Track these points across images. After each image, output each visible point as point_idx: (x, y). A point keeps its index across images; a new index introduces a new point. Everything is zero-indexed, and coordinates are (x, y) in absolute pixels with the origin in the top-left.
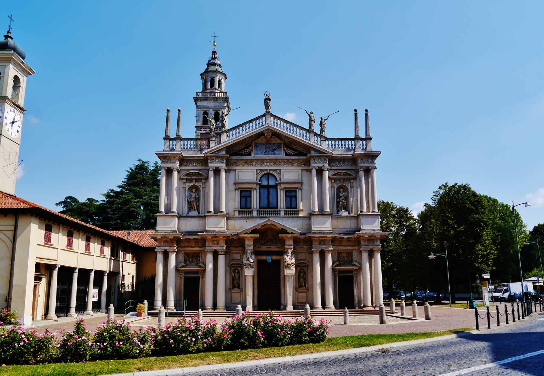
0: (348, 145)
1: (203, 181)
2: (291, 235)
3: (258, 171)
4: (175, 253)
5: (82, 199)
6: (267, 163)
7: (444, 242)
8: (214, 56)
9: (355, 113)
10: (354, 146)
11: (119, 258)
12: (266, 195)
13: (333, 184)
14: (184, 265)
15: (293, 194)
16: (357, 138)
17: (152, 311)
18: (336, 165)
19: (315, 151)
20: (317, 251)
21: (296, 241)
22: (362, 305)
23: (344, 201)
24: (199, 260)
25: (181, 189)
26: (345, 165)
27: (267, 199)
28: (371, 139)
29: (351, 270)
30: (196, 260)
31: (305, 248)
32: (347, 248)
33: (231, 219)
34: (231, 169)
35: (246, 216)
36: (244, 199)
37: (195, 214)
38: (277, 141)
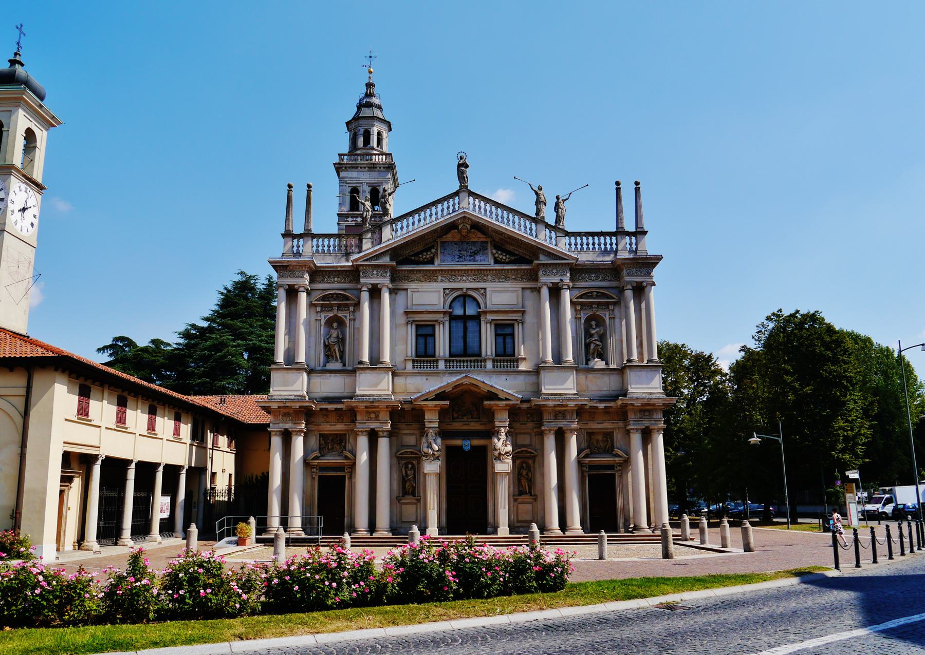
0: (605, 244)
1: (351, 309)
2: (504, 402)
3: (447, 291)
4: (302, 435)
5: (142, 341)
6: (462, 276)
7: (776, 415)
8: (369, 92)
9: (617, 189)
10: (614, 246)
11: (207, 443)
12: (461, 334)
13: (579, 312)
14: (319, 455)
15: (508, 331)
16: (620, 232)
17: (264, 536)
18: (583, 280)
19: (547, 256)
20: (551, 430)
21: (514, 413)
22: (632, 526)
23: (598, 343)
24: (345, 447)
25: (313, 322)
27: (462, 340)
28: (645, 233)
29: (611, 463)
30: (338, 447)
31: (530, 425)
32: (604, 425)
33: (399, 376)
34: (399, 287)
35: (425, 369)
36: (421, 341)
37: (337, 366)
38: (481, 237)
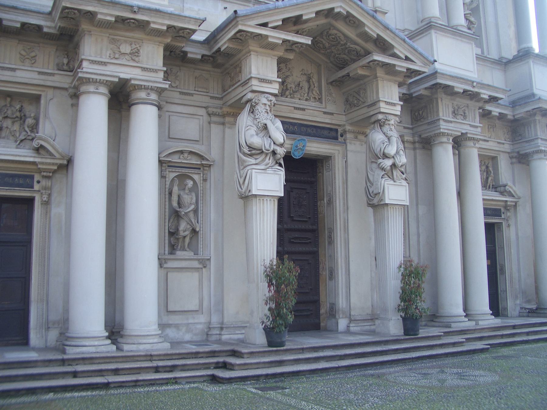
30: (16, 127)
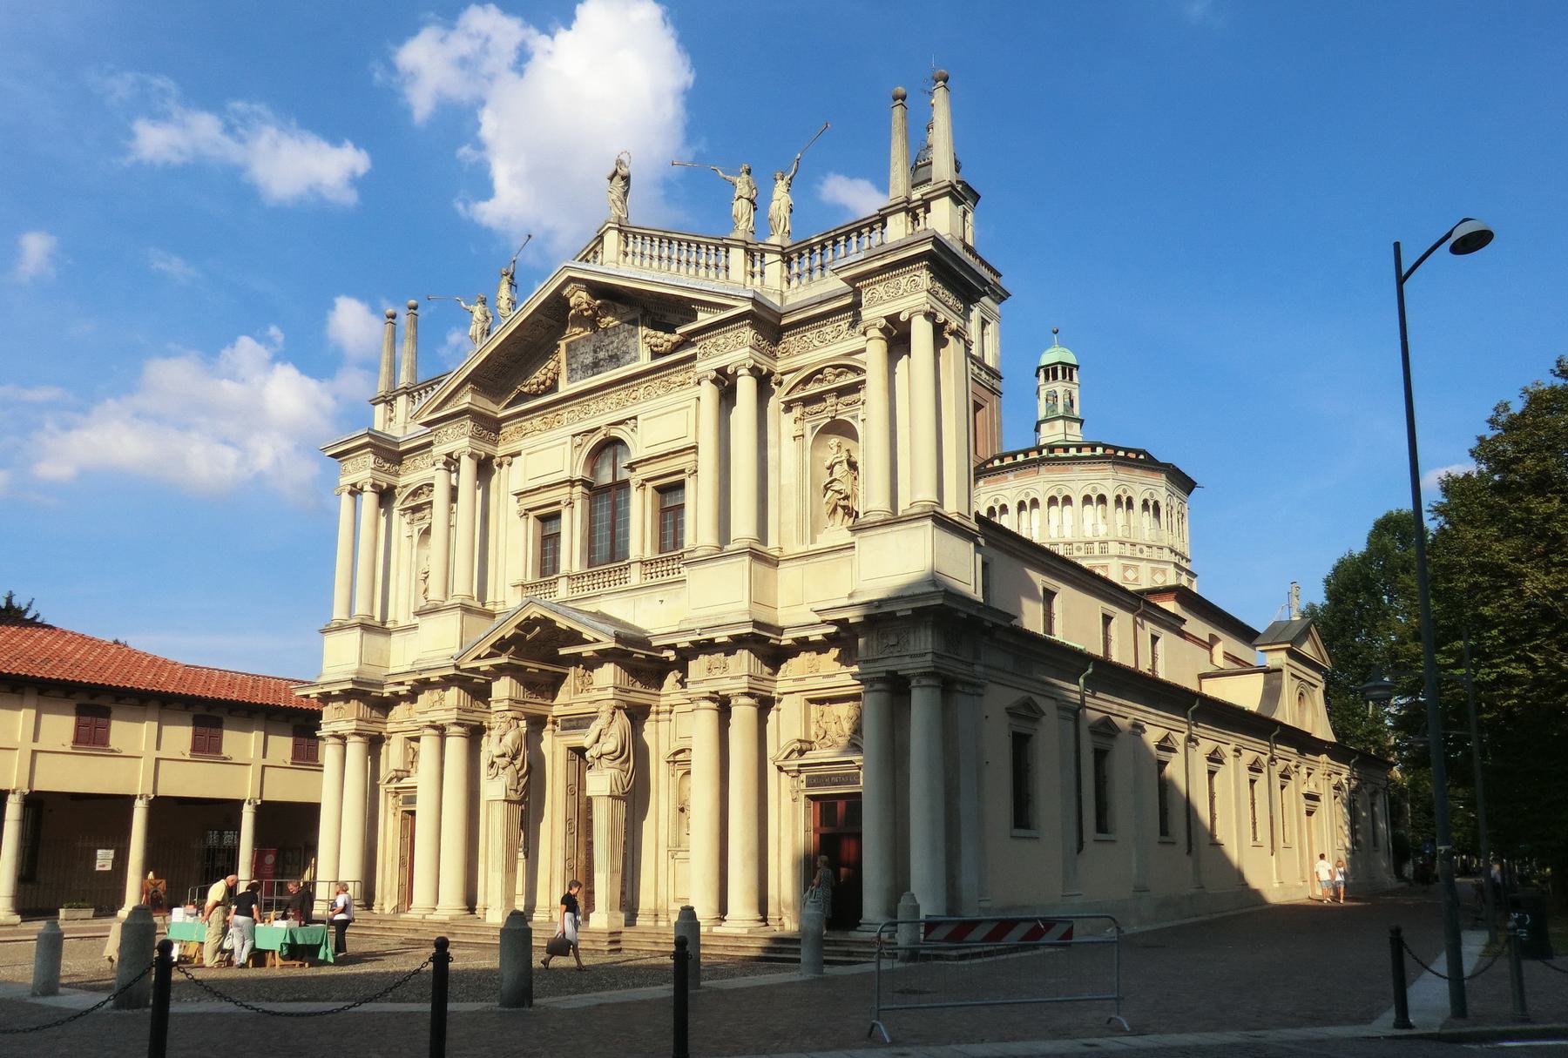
3: (578, 440)
26: (841, 337)
